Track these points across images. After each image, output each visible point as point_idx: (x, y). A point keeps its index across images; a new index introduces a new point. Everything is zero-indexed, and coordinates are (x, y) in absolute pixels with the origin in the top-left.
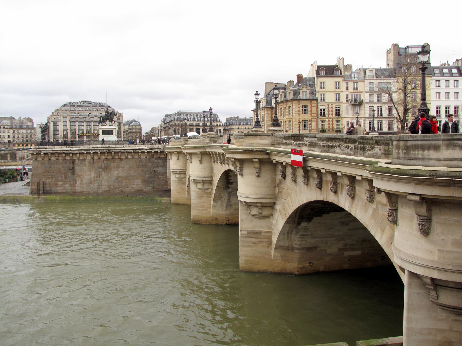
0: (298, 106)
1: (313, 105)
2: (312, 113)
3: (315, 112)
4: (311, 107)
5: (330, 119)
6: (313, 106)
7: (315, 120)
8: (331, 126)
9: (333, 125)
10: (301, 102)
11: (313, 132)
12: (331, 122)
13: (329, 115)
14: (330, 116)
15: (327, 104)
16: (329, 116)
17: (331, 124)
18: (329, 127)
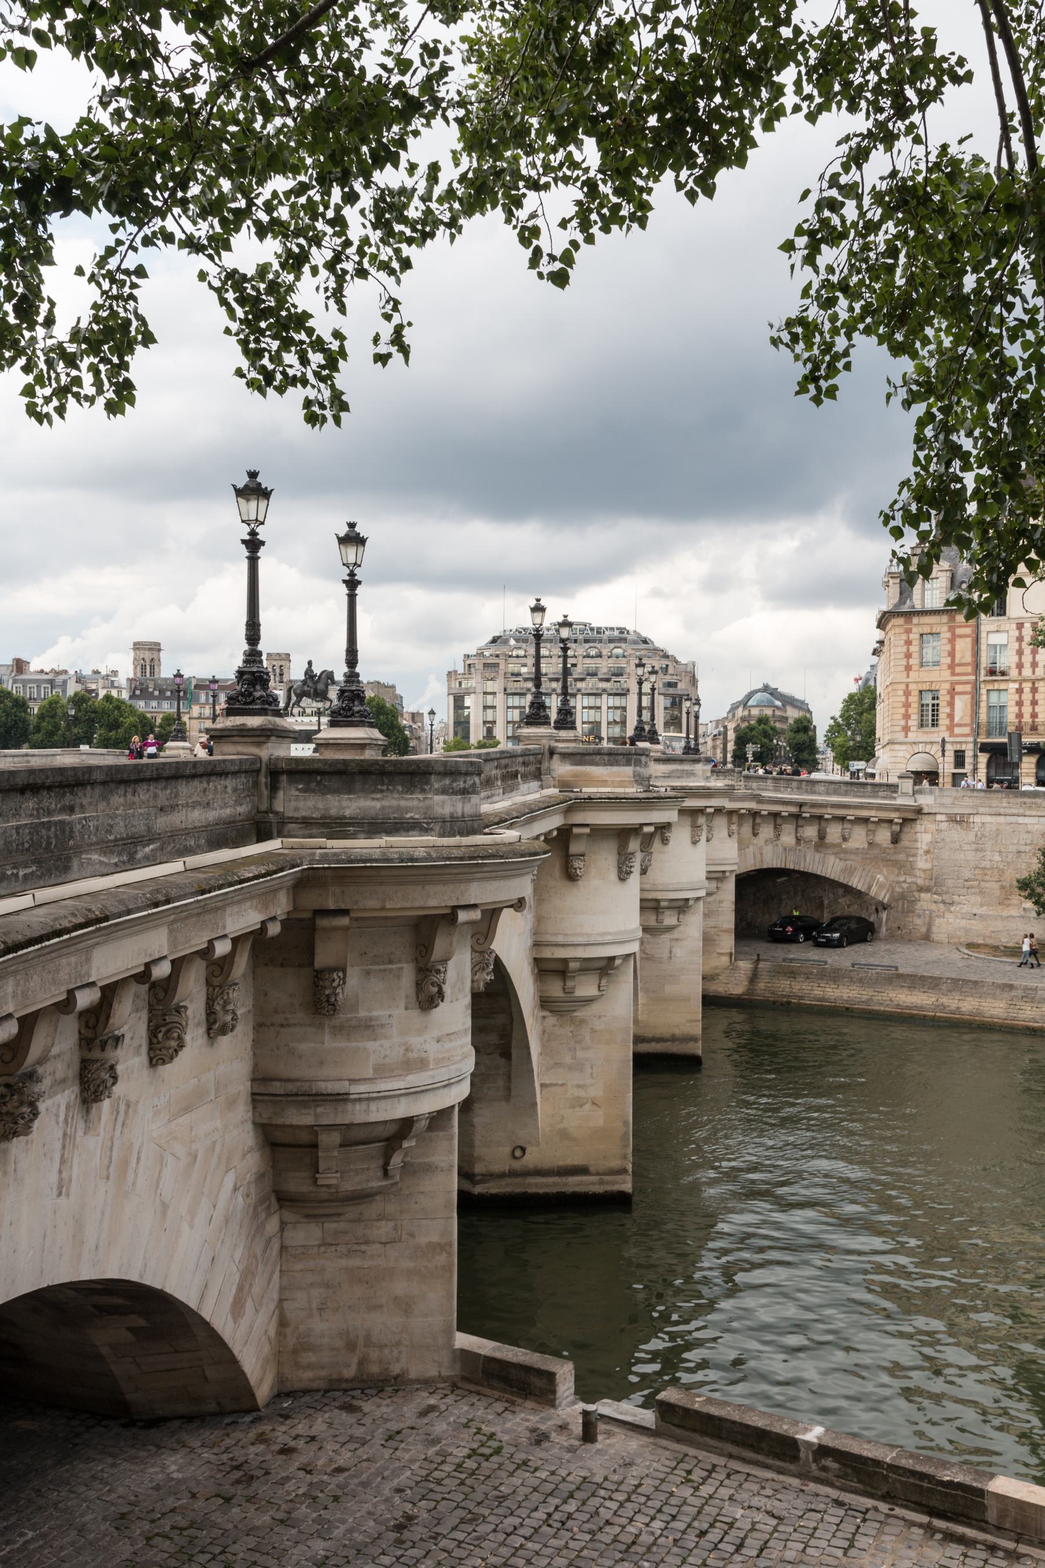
0: (904, 637)
1: (959, 631)
2: (957, 661)
3: (968, 659)
4: (952, 641)
5: (1024, 685)
6: (961, 636)
7: (968, 688)
8: (1027, 710)
9: (1037, 709)
10: (915, 620)
11: (958, 736)
12: (1027, 696)
13: (1020, 666)
14: (1027, 672)
15: (1014, 626)
16: (1020, 673)
17: (1027, 703)
18: (1020, 716)
